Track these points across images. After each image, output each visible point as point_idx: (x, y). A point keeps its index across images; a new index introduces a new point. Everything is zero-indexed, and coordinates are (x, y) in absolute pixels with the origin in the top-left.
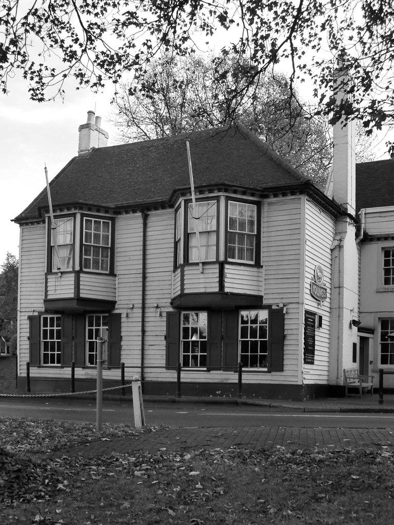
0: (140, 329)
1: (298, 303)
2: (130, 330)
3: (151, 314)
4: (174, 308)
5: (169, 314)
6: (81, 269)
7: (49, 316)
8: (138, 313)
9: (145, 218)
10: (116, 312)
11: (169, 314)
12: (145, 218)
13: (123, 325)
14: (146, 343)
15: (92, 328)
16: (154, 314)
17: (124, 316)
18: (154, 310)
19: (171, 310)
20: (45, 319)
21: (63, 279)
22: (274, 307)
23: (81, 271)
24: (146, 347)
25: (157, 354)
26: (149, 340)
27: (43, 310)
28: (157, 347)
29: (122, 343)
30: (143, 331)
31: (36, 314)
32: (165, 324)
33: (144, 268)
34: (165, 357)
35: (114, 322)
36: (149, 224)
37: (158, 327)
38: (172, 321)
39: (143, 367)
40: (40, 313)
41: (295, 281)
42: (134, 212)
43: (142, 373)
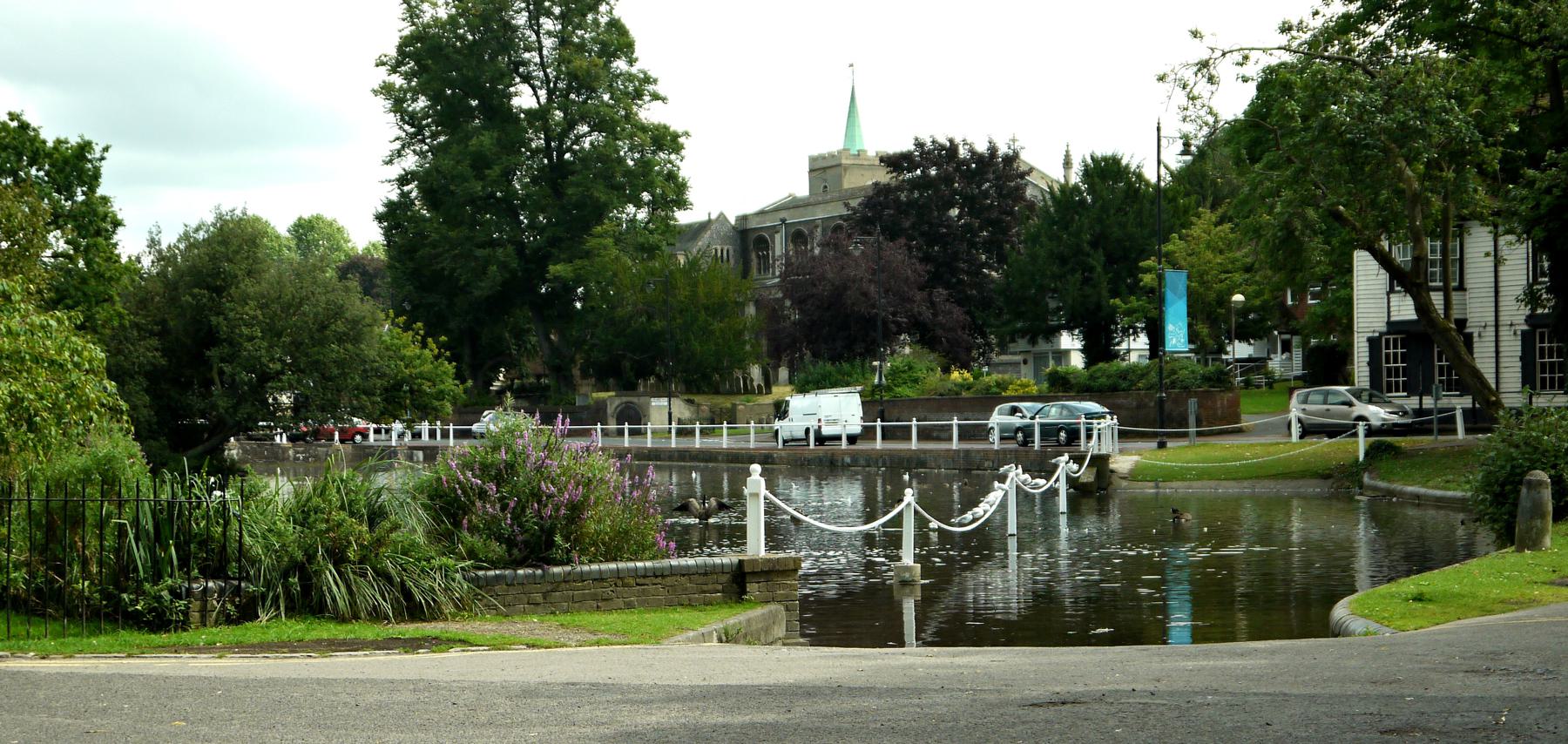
0: (1494, 349)
3: (1505, 333)
4: (1529, 325)
7: (1391, 337)
8: (1491, 331)
13: (1475, 345)
16: (1508, 333)
17: (1475, 335)
18: (1508, 328)
19: (1525, 327)
26: (1504, 362)
30: (1497, 352)
31: (1377, 334)
32: (1520, 343)
33: (1496, 282)
40: (1381, 334)
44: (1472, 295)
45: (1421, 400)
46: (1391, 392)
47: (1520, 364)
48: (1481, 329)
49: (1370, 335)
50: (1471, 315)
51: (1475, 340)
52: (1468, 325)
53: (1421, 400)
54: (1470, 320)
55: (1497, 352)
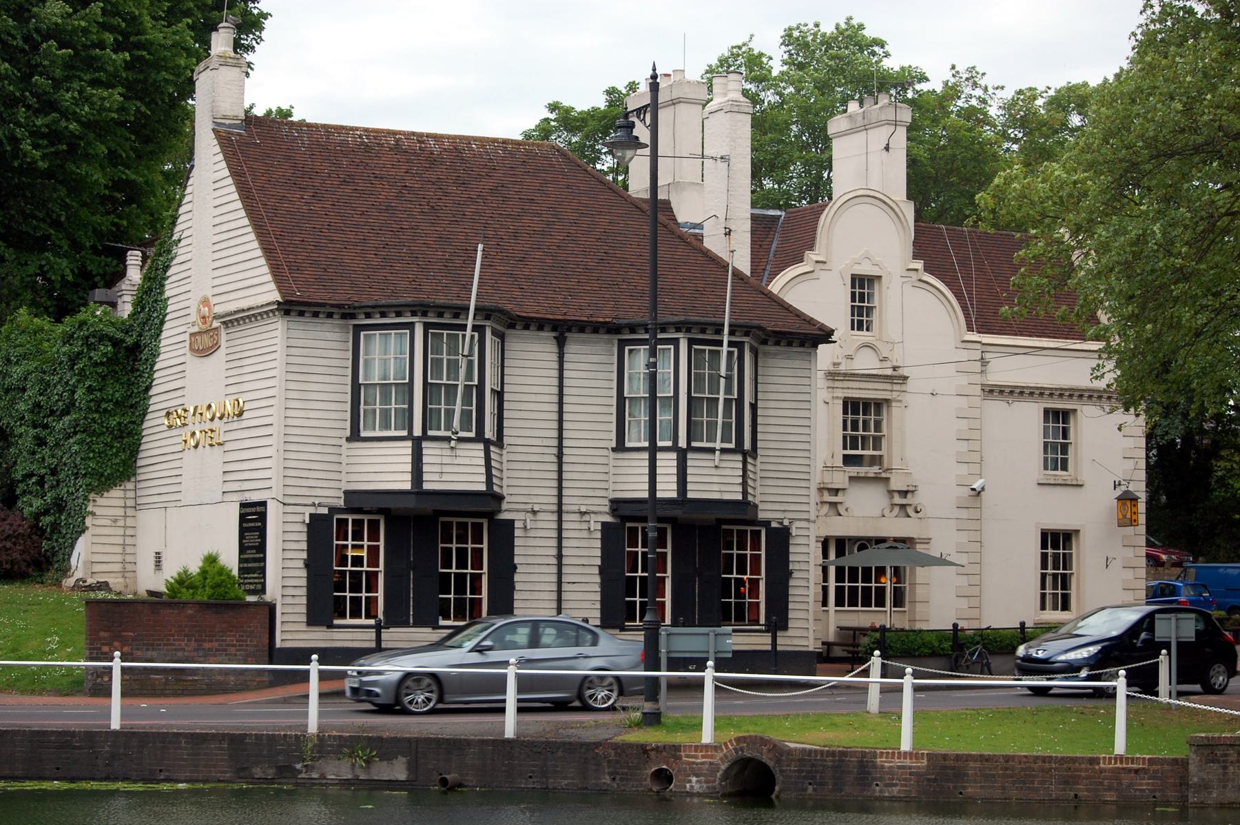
0: (554, 552)
1: (808, 520)
3: (570, 522)
4: (614, 516)
5: (604, 524)
6: (689, 443)
7: (350, 518)
8: (548, 521)
9: (561, 343)
10: (504, 516)
12: (561, 343)
13: (517, 542)
15: (470, 542)
16: (577, 526)
17: (517, 525)
18: (576, 517)
19: (608, 519)
20: (342, 523)
21: (459, 453)
22: (774, 525)
26: (569, 573)
27: (341, 503)
29: (517, 578)
30: (560, 556)
31: (325, 511)
32: (598, 544)
33: (560, 438)
34: (598, 606)
35: (504, 534)
40: (333, 510)
41: (803, 484)
44: (512, 457)
45: (378, 639)
46: (343, 616)
47: (598, 579)
48: (529, 516)
49: (312, 510)
50: (512, 491)
51: (517, 533)
52: (504, 506)
53: (378, 639)
54: (508, 499)
55: (560, 556)
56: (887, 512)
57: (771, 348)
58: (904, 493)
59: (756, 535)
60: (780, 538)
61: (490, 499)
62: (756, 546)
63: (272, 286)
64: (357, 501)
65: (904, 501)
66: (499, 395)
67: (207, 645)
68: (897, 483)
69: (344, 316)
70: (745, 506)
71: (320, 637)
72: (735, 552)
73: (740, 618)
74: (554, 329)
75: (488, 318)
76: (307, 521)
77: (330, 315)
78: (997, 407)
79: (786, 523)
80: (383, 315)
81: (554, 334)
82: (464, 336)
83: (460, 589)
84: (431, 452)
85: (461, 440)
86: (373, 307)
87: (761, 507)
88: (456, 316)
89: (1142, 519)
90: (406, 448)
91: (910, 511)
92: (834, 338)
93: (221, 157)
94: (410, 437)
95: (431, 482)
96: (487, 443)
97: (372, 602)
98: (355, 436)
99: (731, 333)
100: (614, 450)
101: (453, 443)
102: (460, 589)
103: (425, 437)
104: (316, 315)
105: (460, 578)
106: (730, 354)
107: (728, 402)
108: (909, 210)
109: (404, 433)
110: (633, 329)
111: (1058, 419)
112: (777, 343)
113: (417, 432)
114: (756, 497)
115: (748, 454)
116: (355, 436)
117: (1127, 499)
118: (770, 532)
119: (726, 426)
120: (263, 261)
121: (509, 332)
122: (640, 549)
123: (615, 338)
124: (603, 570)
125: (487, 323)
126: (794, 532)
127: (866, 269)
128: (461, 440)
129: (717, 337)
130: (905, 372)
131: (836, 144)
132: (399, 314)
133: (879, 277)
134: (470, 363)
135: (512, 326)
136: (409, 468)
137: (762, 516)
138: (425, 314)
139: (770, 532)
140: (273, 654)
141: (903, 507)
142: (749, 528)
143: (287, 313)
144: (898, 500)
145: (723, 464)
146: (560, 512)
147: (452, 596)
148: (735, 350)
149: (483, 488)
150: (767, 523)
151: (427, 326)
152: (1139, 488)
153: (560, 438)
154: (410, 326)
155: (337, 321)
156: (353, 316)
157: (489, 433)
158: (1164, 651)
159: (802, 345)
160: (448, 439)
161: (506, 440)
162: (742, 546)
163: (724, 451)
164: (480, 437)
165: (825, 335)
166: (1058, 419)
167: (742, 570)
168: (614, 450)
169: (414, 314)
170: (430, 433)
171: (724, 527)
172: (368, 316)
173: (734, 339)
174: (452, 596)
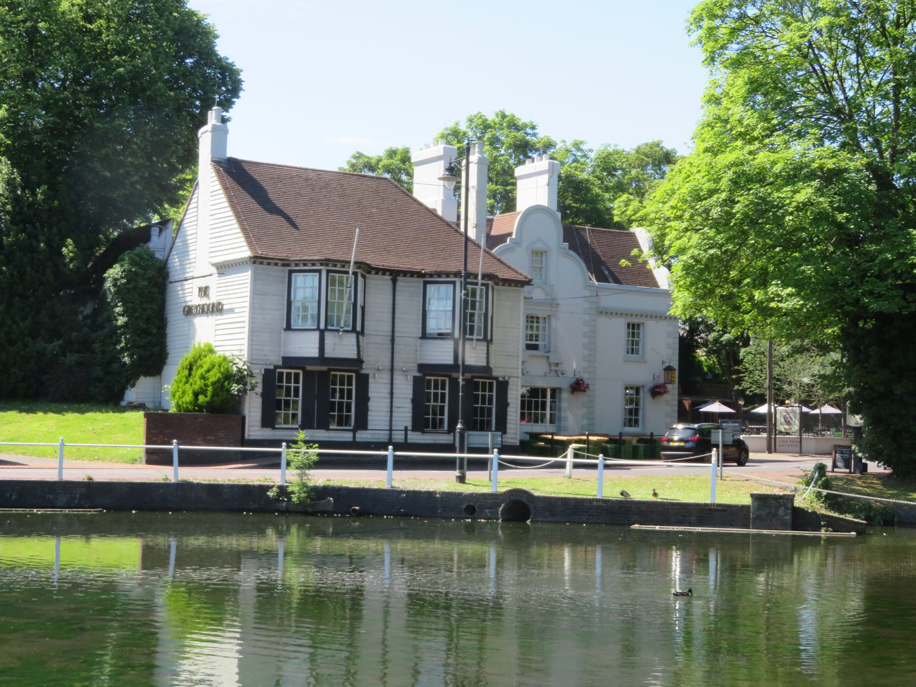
2: (377, 391)
7: (285, 371)
9: (394, 281)
10: (364, 372)
11: (416, 379)
12: (394, 281)
14: (394, 404)
17: (371, 376)
19: (418, 374)
22: (500, 379)
23: (326, 329)
24: (394, 409)
25: (404, 416)
27: (280, 363)
28: (403, 410)
30: (392, 393)
33: (393, 331)
35: (363, 382)
36: (398, 288)
37: (405, 390)
38: (418, 384)
39: (391, 430)
40: (276, 367)
42: (384, 274)
43: (391, 435)
45: (354, 437)
49: (266, 367)
52: (364, 366)
53: (354, 437)
56: (548, 374)
57: (500, 287)
58: (557, 364)
59: (491, 384)
60: (503, 386)
61: (359, 361)
62: (491, 390)
63: (247, 248)
64: (289, 362)
65: (556, 369)
66: (363, 308)
67: (209, 438)
68: (553, 359)
69: (284, 265)
70: (486, 370)
71: (268, 434)
72: (480, 393)
73: (482, 429)
74: (391, 275)
75: (359, 268)
76: (263, 373)
77: (276, 264)
78: (603, 321)
79: (506, 378)
80: (305, 265)
81: (391, 277)
82: (347, 278)
83: (341, 410)
84: (328, 337)
85: (345, 331)
86: (300, 260)
87: (494, 369)
88: (343, 266)
89: (677, 380)
90: (316, 336)
91: (560, 374)
92: (532, 283)
93: (216, 178)
94: (318, 329)
95: (329, 353)
96: (358, 334)
97: (294, 416)
98: (288, 328)
99: (483, 278)
100: (420, 338)
101: (341, 333)
102: (341, 410)
103: (326, 329)
104: (269, 264)
105: (340, 404)
106: (482, 290)
107: (480, 315)
108: (559, 215)
109: (315, 327)
110: (431, 276)
111: (634, 329)
112: (504, 285)
113: (322, 326)
114: (492, 365)
115: (488, 340)
116: (288, 328)
117: (669, 369)
118: (499, 382)
119: (479, 328)
120: (241, 235)
121: (368, 275)
122: (432, 391)
123: (422, 280)
124: (414, 401)
125: (359, 271)
126: (510, 383)
127: (539, 246)
128: (345, 331)
129: (475, 281)
130: (559, 301)
131: (520, 183)
132: (313, 265)
133: (546, 252)
134: (350, 291)
135: (369, 273)
136: (317, 345)
137: (495, 374)
138: (327, 265)
139: (499, 382)
140: (244, 443)
141: (556, 371)
142: (488, 381)
143: (254, 262)
144: (553, 368)
145: (478, 348)
146: (392, 370)
147: (336, 413)
148: (484, 288)
149: (355, 357)
150: (496, 379)
151: (328, 272)
152: (675, 364)
153: (393, 331)
154: (319, 271)
155: (280, 268)
156: (288, 265)
157: (359, 328)
158: (714, 449)
159: (516, 286)
160: (338, 331)
161: (366, 332)
162: (484, 390)
163: (478, 340)
164: (354, 330)
165: (528, 282)
166: (634, 329)
167: (483, 402)
168: (420, 338)
169: (322, 265)
170: (329, 327)
171: (475, 380)
172: (297, 265)
173: (484, 282)
174: (336, 413)
